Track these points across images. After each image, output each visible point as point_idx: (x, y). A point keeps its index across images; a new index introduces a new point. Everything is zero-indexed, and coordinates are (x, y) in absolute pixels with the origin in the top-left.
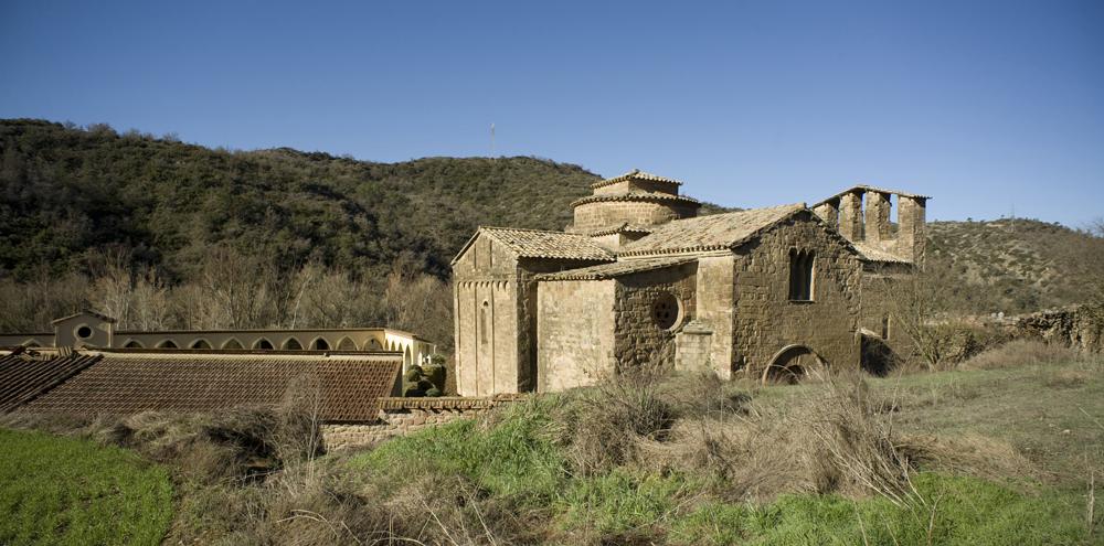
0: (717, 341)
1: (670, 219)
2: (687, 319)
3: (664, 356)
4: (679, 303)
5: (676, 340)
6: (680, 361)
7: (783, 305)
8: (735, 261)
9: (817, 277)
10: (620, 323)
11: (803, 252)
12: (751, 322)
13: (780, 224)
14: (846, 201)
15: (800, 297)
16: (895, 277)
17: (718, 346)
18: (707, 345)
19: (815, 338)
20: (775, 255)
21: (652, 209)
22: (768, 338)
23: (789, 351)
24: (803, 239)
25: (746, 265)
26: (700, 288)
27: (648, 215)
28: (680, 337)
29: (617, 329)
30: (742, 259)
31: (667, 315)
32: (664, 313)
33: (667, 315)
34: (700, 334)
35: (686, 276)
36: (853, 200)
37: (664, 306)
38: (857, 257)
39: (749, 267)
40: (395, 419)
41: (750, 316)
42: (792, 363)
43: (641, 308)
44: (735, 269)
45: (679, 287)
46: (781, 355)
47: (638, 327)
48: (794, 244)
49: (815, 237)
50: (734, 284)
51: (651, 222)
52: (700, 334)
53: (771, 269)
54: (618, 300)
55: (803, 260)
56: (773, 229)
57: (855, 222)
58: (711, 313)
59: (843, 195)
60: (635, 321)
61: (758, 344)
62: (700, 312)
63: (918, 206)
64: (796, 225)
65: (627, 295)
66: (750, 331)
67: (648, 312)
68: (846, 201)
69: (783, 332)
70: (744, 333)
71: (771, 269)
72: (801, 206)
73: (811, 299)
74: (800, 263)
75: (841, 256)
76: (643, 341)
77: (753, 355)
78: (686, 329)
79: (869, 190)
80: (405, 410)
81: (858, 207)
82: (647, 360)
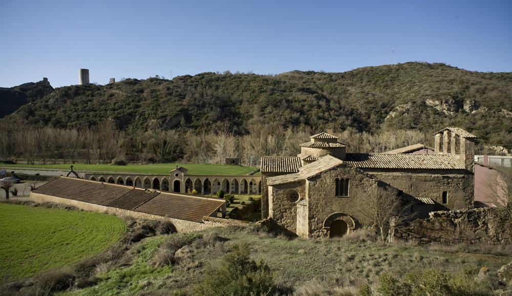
1: (327, 154)
2: (302, 199)
8: (309, 183)
9: (351, 187)
11: (342, 180)
13: (330, 170)
16: (450, 175)
20: (328, 181)
29: (273, 202)
30: (312, 183)
31: (295, 197)
32: (293, 197)
33: (295, 197)
35: (301, 185)
39: (316, 185)
40: (206, 222)
41: (316, 202)
42: (338, 219)
45: (299, 189)
46: (331, 216)
50: (309, 191)
53: (326, 186)
54: (273, 193)
56: (327, 172)
60: (280, 199)
61: (321, 211)
63: (468, 142)
64: (338, 169)
65: (277, 191)
66: (317, 207)
71: (326, 186)
75: (365, 179)
76: (284, 206)
80: (207, 220)
82: (286, 212)
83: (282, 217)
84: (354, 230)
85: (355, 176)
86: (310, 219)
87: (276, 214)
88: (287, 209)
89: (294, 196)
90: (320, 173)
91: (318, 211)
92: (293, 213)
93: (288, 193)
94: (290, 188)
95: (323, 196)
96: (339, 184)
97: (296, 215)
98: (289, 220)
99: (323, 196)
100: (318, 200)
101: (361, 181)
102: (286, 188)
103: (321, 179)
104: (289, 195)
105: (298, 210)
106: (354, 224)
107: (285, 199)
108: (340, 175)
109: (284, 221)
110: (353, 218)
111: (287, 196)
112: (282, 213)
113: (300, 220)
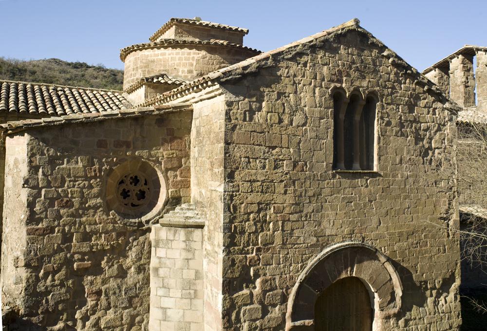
0: (209, 239)
2: (174, 202)
3: (129, 261)
5: (152, 236)
6: (156, 270)
7: (323, 178)
8: (229, 104)
9: (383, 134)
10: (37, 208)
11: (356, 95)
12: (262, 207)
14: (456, 64)
15: (357, 165)
17: (209, 247)
18: (196, 246)
19: (382, 229)
20: (306, 98)
21: (196, 57)
22: (297, 233)
23: (335, 254)
24: (354, 74)
25: (252, 112)
26: (194, 152)
27: (192, 65)
28: (157, 231)
29: (32, 219)
30: (244, 103)
31: (142, 195)
32: (135, 195)
34: (185, 227)
36: (463, 63)
37: (136, 181)
38: (447, 105)
39: (258, 116)
43: (81, 183)
44: (228, 117)
45: (163, 152)
46: (321, 264)
47: (72, 215)
48: (340, 81)
49: (376, 72)
50: (227, 143)
51: (195, 73)
52: (185, 227)
53: (298, 119)
54: (33, 169)
55: (359, 110)
56: (300, 54)
57: (466, 87)
58: (203, 191)
59: (452, 58)
60: (69, 204)
61: (278, 241)
62: (195, 191)
64: (342, 51)
65: (53, 162)
66: (262, 224)
67: (96, 190)
68: (456, 64)
69: (325, 223)
70: (250, 227)
71: (298, 119)
72: (350, 23)
73: (375, 169)
74: (352, 118)
75: (422, 103)
76: (86, 237)
77: (268, 264)
78: (168, 218)
79: (478, 50)
81: (469, 70)
82: (96, 270)
83: (77, 298)
84: (398, 316)
85: (393, 88)
86: (230, 286)
87: (41, 288)
88: (103, 252)
89: (134, 190)
90: (277, 57)
91: (268, 244)
92: (132, 277)
93: (110, 172)
94: (118, 144)
95: (286, 166)
96: (344, 108)
98: (111, 314)
99: (286, 166)
100: (267, 187)
101: (411, 107)
102: (101, 144)
103: (279, 87)
104: (112, 182)
105: (157, 255)
106: (399, 292)
107: (92, 202)
108: (348, 75)
109: (85, 318)
110: (396, 265)
111: (104, 184)
113: (167, 303)
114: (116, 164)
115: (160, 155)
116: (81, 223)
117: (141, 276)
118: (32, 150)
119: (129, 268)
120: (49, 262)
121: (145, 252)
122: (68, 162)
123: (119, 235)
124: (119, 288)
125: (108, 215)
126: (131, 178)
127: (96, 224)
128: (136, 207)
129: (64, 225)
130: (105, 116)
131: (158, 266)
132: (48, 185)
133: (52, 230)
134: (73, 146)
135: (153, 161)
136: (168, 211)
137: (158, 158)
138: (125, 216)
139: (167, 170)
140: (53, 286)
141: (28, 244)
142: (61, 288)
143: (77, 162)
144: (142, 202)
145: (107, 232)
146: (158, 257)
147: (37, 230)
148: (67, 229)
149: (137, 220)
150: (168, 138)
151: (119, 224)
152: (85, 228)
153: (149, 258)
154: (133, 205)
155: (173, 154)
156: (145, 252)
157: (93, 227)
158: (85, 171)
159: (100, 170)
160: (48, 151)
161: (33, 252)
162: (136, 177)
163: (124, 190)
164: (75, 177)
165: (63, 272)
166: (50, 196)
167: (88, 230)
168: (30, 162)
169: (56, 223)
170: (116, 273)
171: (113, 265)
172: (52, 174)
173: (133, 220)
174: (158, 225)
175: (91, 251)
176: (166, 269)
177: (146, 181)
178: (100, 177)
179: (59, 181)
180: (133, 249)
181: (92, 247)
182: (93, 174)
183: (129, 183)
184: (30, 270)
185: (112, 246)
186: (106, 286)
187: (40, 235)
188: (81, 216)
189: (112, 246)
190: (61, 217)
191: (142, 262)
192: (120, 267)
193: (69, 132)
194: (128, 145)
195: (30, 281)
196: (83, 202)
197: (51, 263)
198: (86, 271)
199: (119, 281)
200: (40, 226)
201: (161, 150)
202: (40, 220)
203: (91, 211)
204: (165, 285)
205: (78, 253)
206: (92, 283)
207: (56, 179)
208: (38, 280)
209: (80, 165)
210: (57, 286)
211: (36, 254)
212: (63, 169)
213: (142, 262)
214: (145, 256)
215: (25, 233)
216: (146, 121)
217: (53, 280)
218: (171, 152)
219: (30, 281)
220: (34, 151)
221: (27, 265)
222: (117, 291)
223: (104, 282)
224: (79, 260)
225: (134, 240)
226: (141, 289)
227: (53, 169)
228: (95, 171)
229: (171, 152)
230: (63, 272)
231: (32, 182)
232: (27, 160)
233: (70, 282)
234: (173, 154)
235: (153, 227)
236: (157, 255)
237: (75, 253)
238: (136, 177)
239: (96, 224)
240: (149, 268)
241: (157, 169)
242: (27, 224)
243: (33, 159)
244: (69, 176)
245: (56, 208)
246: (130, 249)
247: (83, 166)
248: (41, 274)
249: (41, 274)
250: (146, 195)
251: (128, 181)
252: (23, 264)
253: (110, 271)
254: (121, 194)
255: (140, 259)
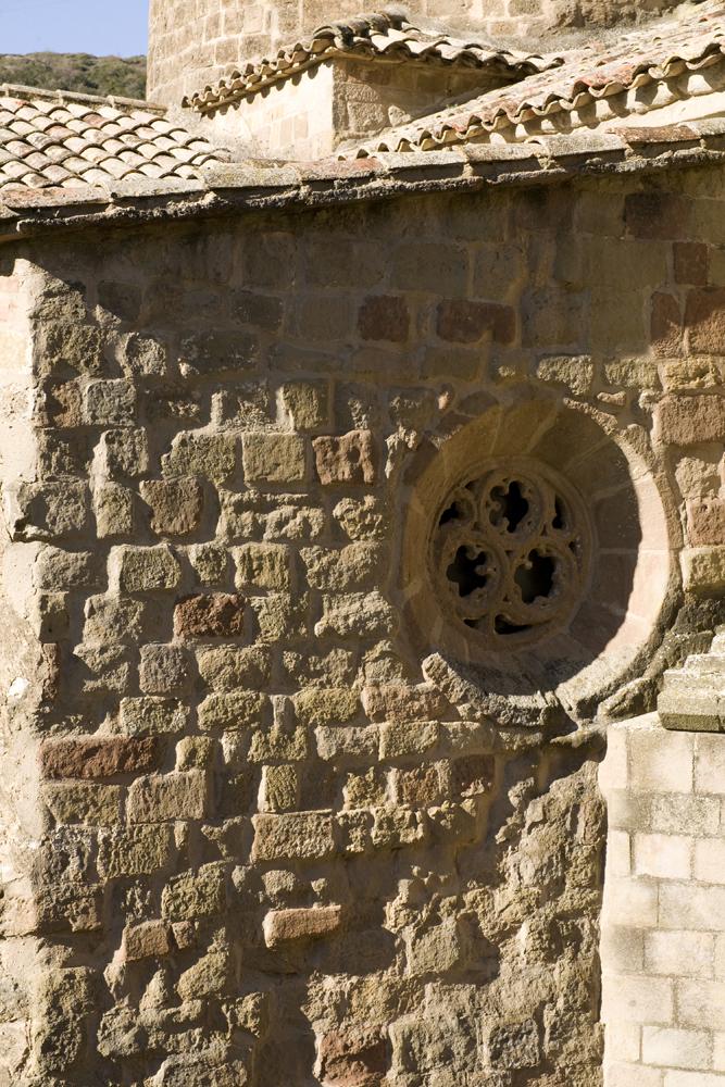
3: (504, 896)
4: (644, 480)
5: (609, 778)
6: (637, 940)
10: (91, 643)
29: (68, 697)
31: (540, 577)
37: (514, 506)
43: (289, 516)
47: (252, 678)
54: (66, 445)
60: (234, 625)
65: (158, 407)
67: (357, 553)
76: (316, 785)
82: (361, 945)
87: (116, 1038)
88: (392, 857)
89: (509, 551)
92: (523, 981)
93: (418, 461)
94: (456, 322)
97: (588, 996)
102: (381, 320)
104: (421, 509)
112: (281, 971)
114: (447, 422)
115: (642, 377)
116: (292, 719)
117: (561, 971)
118: (55, 345)
119: (508, 932)
120: (152, 911)
121: (580, 854)
122: (229, 410)
123: (462, 774)
124: (466, 1027)
125: (413, 676)
126: (496, 491)
127: (358, 718)
128: (516, 637)
129: (217, 728)
130: (399, 173)
131: (649, 920)
132: (140, 528)
133: (160, 756)
134: (251, 329)
135: (613, 408)
136: (677, 656)
137: (637, 388)
138: (485, 679)
139: (675, 452)
140: (170, 1026)
141: (52, 822)
142: (206, 1036)
143: (270, 414)
144: (541, 609)
145: (409, 761)
146: (642, 878)
147: (91, 752)
148: (227, 744)
149: (539, 701)
150: (681, 293)
151: (465, 723)
152: (311, 740)
153: (597, 881)
154: (505, 628)
155: (701, 373)
156: (580, 854)
157: (347, 733)
158: (308, 455)
159: (377, 453)
160: (133, 351)
161: (73, 866)
162: (516, 487)
163: (463, 550)
164: (261, 484)
165: (215, 957)
166: (148, 581)
167: (324, 749)
168: (52, 408)
169: (179, 717)
170: (448, 956)
171: (435, 920)
172: (153, 473)
173: (524, 702)
174: (648, 722)
175: (340, 855)
176: (692, 937)
177: (558, 507)
178: (376, 486)
179: (190, 506)
180: (525, 840)
181: (342, 833)
182: (345, 471)
183: (486, 521)
184: (61, 953)
185: (432, 826)
186: (407, 1021)
187: (103, 779)
188: (290, 684)
189: (432, 826)
190: (201, 687)
191: (564, 902)
192: (469, 925)
193: (228, 253)
194: (498, 323)
195: (67, 1004)
196: (304, 600)
197: (159, 917)
198: (313, 952)
199: (463, 994)
200: (104, 732)
201: (653, 352)
202: (106, 704)
203: (338, 658)
204: (688, 1011)
205: (281, 863)
206: (342, 1008)
207: (172, 495)
208: (100, 997)
209: (286, 424)
210: (188, 1024)
211: (89, 875)
212: (207, 443)
213: (564, 902)
214: (579, 874)
215: (33, 768)
216: (583, 208)
217: (171, 998)
218: (693, 363)
219: (67, 1004)
220: (68, 352)
221: (51, 930)
222: (459, 1045)
223: (397, 1003)
224: (287, 898)
225: (532, 794)
226: (561, 1031)
227: (159, 447)
228: (353, 455)
229: (693, 363)
230: (215, 957)
231: (62, 514)
232: (31, 398)
233: (249, 1004)
234: (701, 373)
235: (617, 735)
236: (641, 869)
237: (265, 865)
238: (516, 487)
239: (358, 718)
240: (594, 932)
241: (627, 449)
242: (44, 722)
243: (61, 394)
244: (234, 481)
245: (176, 641)
246: (513, 839)
247: (305, 434)
248: (113, 971)
249: (113, 971)
250: (559, 570)
251: (483, 507)
252: (30, 921)
253: (427, 949)
254: (451, 574)
255: (558, 886)
